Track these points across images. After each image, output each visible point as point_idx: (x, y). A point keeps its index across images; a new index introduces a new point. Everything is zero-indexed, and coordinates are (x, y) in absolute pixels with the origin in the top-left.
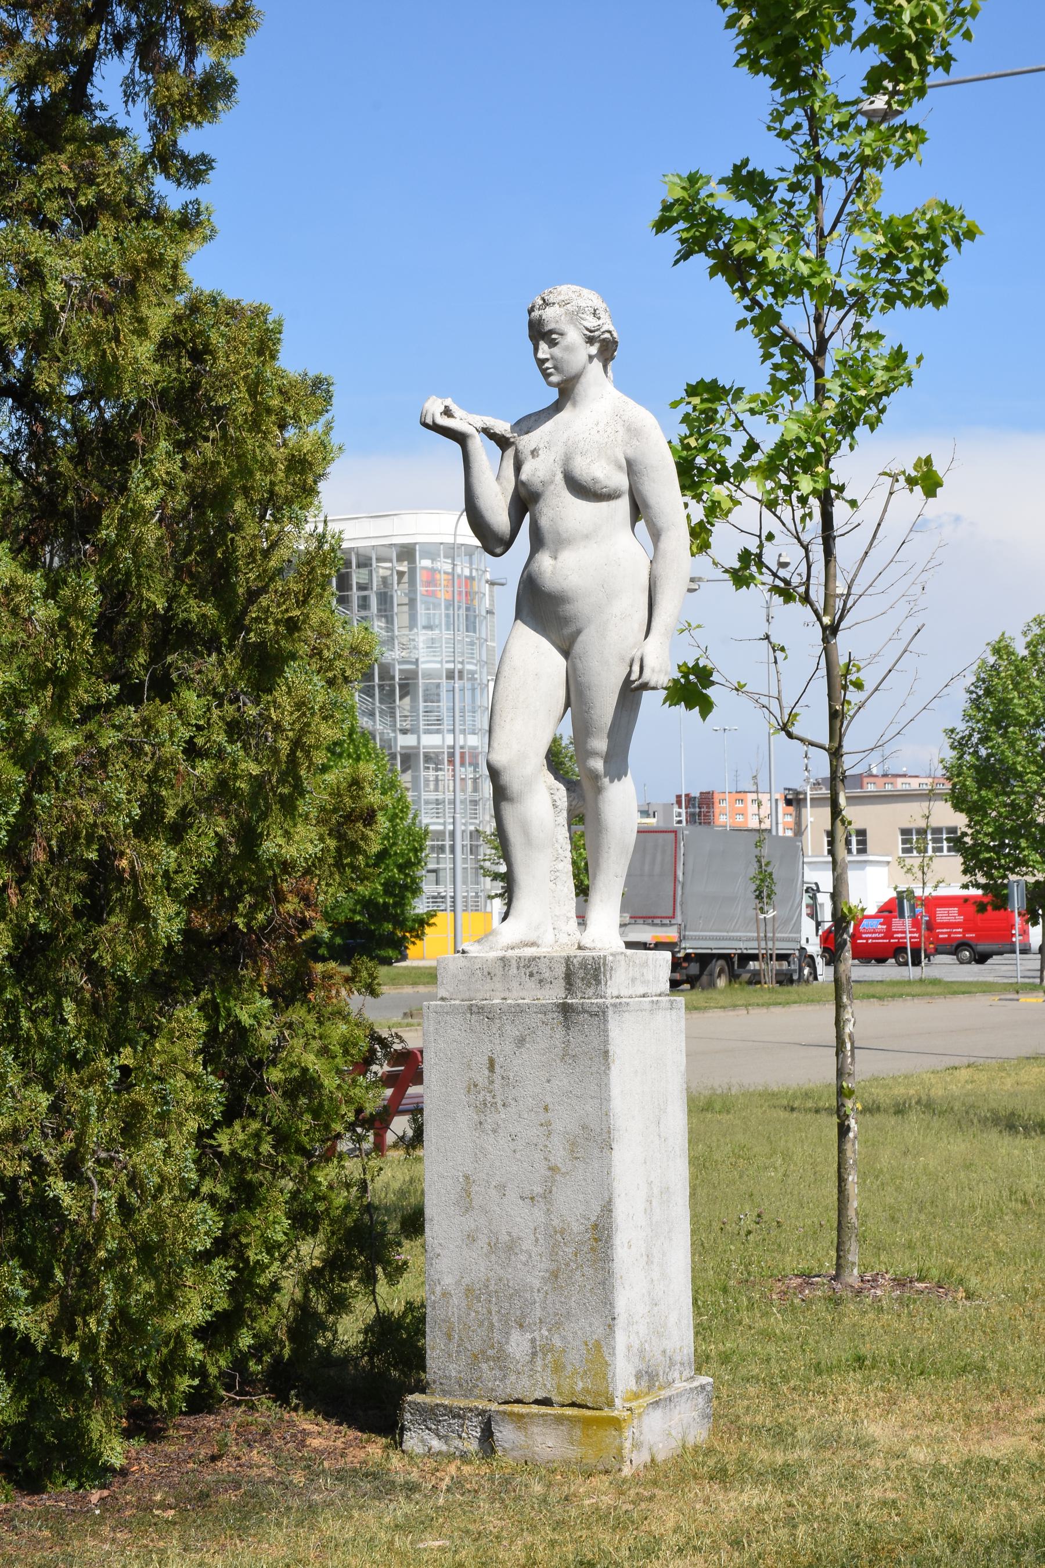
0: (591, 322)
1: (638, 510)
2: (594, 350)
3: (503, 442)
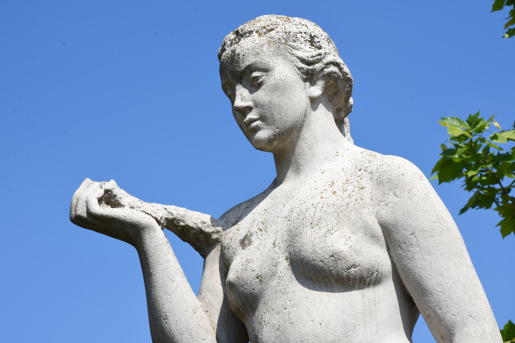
0: (307, 52)
1: (412, 305)
2: (317, 90)
3: (200, 242)
